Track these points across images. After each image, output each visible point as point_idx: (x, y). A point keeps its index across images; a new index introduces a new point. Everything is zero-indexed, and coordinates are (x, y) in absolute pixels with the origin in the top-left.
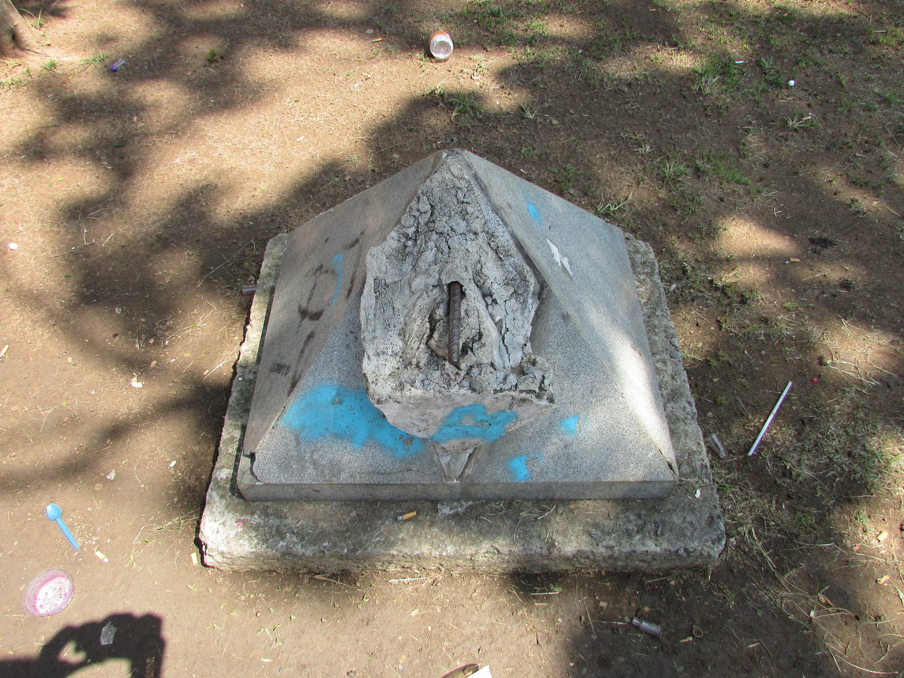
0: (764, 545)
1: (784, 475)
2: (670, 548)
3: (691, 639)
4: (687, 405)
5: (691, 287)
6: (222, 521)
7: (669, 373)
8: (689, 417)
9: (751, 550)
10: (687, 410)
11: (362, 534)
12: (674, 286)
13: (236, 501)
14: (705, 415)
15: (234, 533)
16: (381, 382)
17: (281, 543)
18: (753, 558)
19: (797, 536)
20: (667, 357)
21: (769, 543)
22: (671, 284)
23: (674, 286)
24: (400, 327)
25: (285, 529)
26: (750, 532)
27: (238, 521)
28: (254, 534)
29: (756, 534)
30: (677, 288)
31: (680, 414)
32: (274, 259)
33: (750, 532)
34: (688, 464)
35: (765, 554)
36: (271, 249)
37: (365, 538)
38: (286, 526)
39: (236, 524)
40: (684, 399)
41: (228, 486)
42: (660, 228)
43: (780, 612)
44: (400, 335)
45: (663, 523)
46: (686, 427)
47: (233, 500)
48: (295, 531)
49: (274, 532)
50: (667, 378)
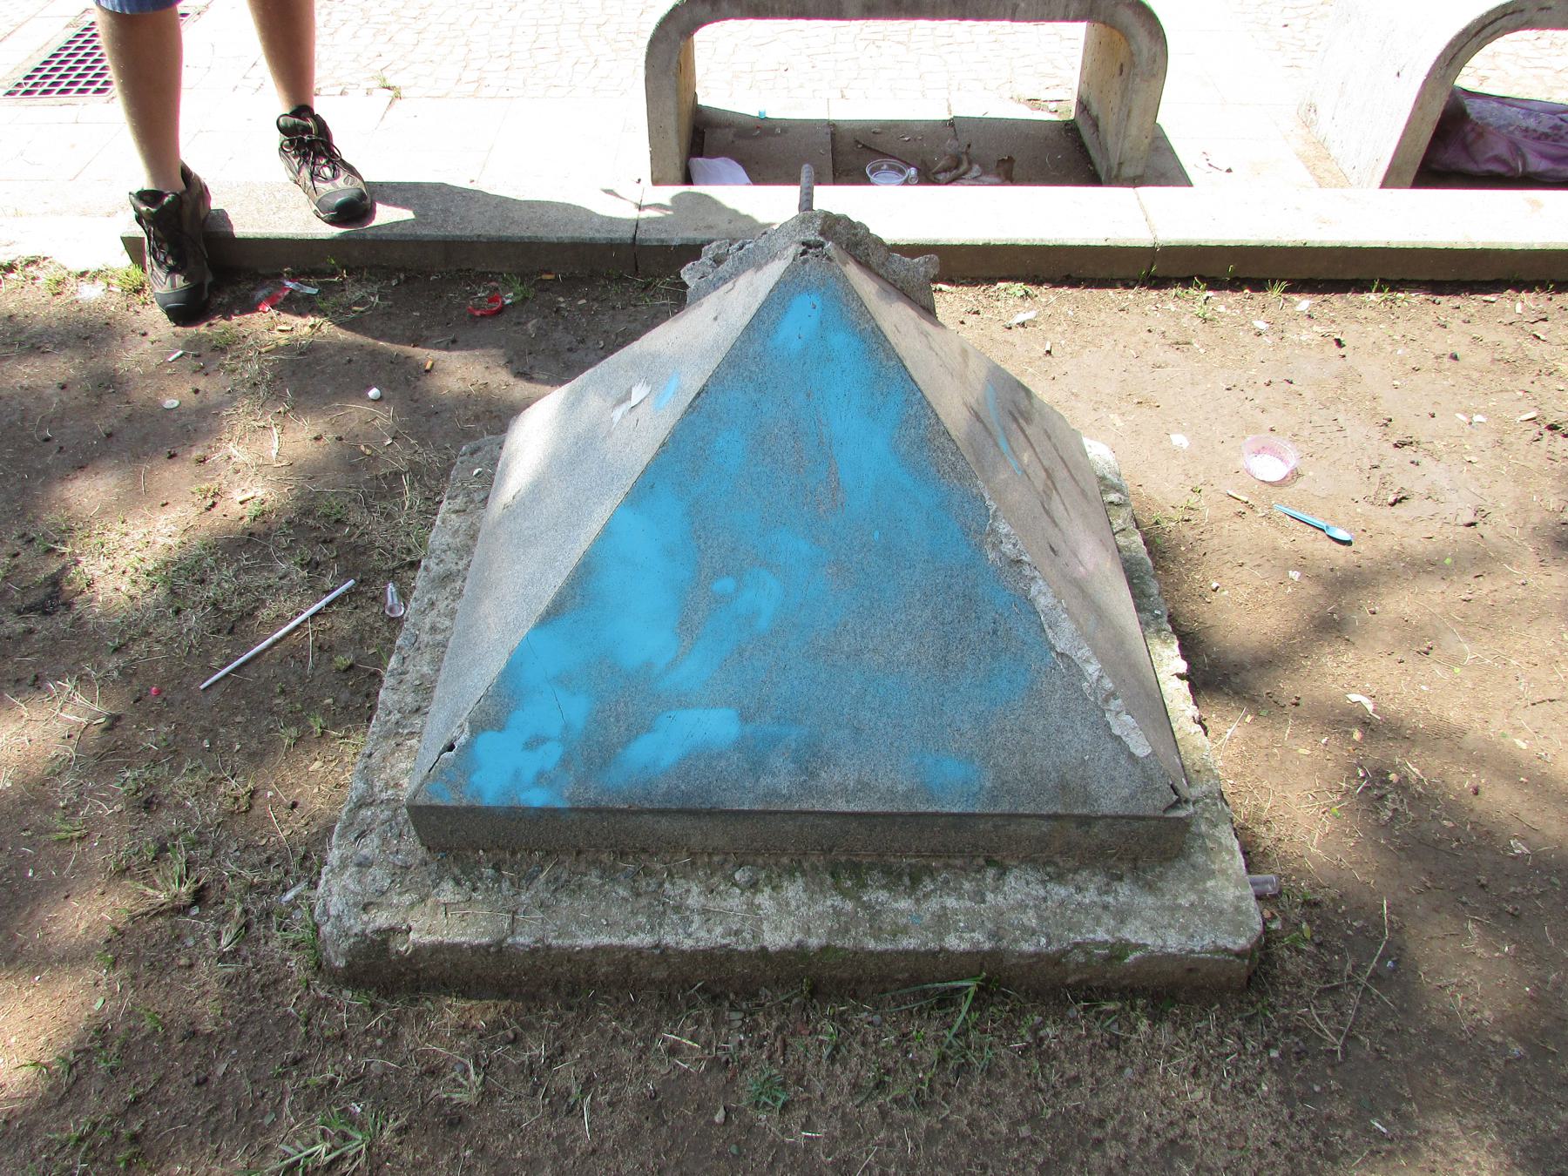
1: (318, 564)
5: (251, 887)
19: (355, 500)
20: (425, 638)
22: (293, 905)
23: (290, 895)
30: (285, 890)
32: (1223, 872)
34: (472, 501)
36: (1241, 898)
42: (222, 1069)
50: (441, 605)
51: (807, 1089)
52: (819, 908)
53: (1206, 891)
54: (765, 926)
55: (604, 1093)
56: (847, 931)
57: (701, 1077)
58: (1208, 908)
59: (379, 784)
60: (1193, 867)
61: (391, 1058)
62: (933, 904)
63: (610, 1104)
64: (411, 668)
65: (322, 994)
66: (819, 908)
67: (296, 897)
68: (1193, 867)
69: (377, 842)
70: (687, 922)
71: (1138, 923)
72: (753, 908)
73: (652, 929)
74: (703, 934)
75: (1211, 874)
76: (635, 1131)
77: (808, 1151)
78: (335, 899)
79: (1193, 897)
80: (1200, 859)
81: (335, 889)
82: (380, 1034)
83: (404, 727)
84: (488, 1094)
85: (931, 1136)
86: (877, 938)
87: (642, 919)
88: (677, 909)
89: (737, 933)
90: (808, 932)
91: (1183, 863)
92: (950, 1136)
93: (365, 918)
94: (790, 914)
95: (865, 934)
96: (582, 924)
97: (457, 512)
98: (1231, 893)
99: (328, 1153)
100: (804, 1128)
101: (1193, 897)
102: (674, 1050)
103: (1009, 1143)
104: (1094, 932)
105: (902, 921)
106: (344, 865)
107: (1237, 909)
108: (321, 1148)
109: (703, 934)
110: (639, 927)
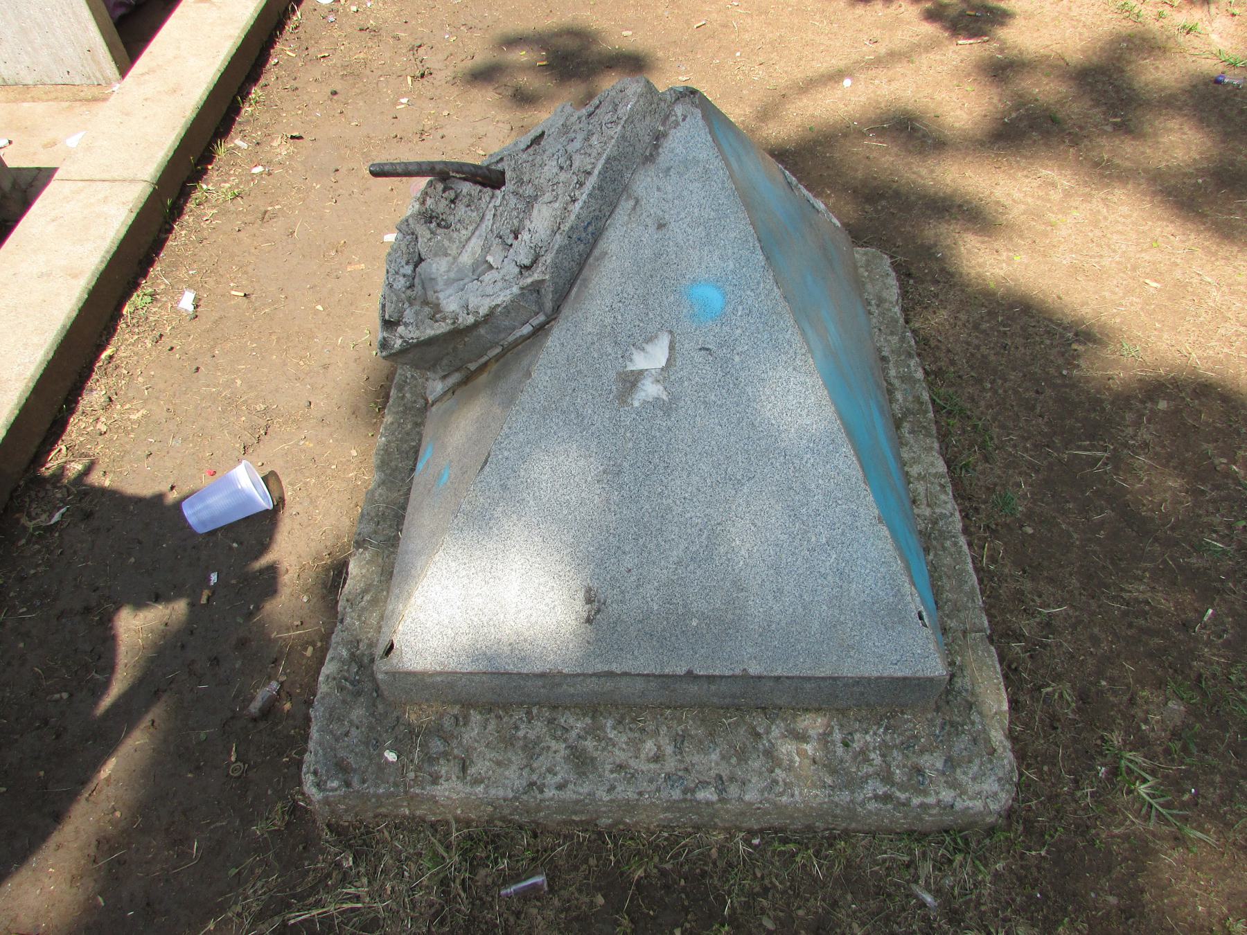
0: (331, 917)
2: (318, 696)
3: (233, 759)
4: (558, 779)
7: (632, 763)
8: (534, 777)
9: (328, 890)
10: (549, 776)
12: (928, 898)
14: (599, 889)
18: (313, 890)
20: (671, 764)
21: (331, 927)
22: (938, 893)
23: (928, 898)
26: (358, 898)
29: (353, 910)
30: (923, 905)
31: (542, 763)
33: (358, 898)
34: (445, 754)
35: (314, 912)
40: (572, 777)
43: (222, 908)
45: (358, 694)
46: (514, 767)
51: (995, 485)
52: (912, 441)
54: (933, 471)
55: (1033, 601)
57: (1005, 544)
59: (866, 769)
61: (1055, 756)
62: (896, 382)
63: (1040, 596)
64: (713, 773)
65: (1021, 828)
66: (912, 441)
67: (927, 888)
69: (926, 757)
70: (942, 516)
72: (920, 477)
74: (949, 506)
76: (1051, 580)
77: (1031, 485)
78: (986, 787)
81: (977, 788)
82: (1040, 771)
83: (792, 761)
84: (1058, 678)
85: (1002, 427)
86: (926, 412)
87: (948, 544)
88: (935, 523)
89: (943, 486)
90: (931, 448)
92: (1001, 418)
93: (1000, 750)
94: (919, 456)
96: (962, 582)
97: (464, 769)
99: (1144, 781)
102: (993, 559)
103: (996, 392)
105: (910, 398)
106: (953, 785)
108: (1142, 789)
109: (949, 506)
110: (955, 544)
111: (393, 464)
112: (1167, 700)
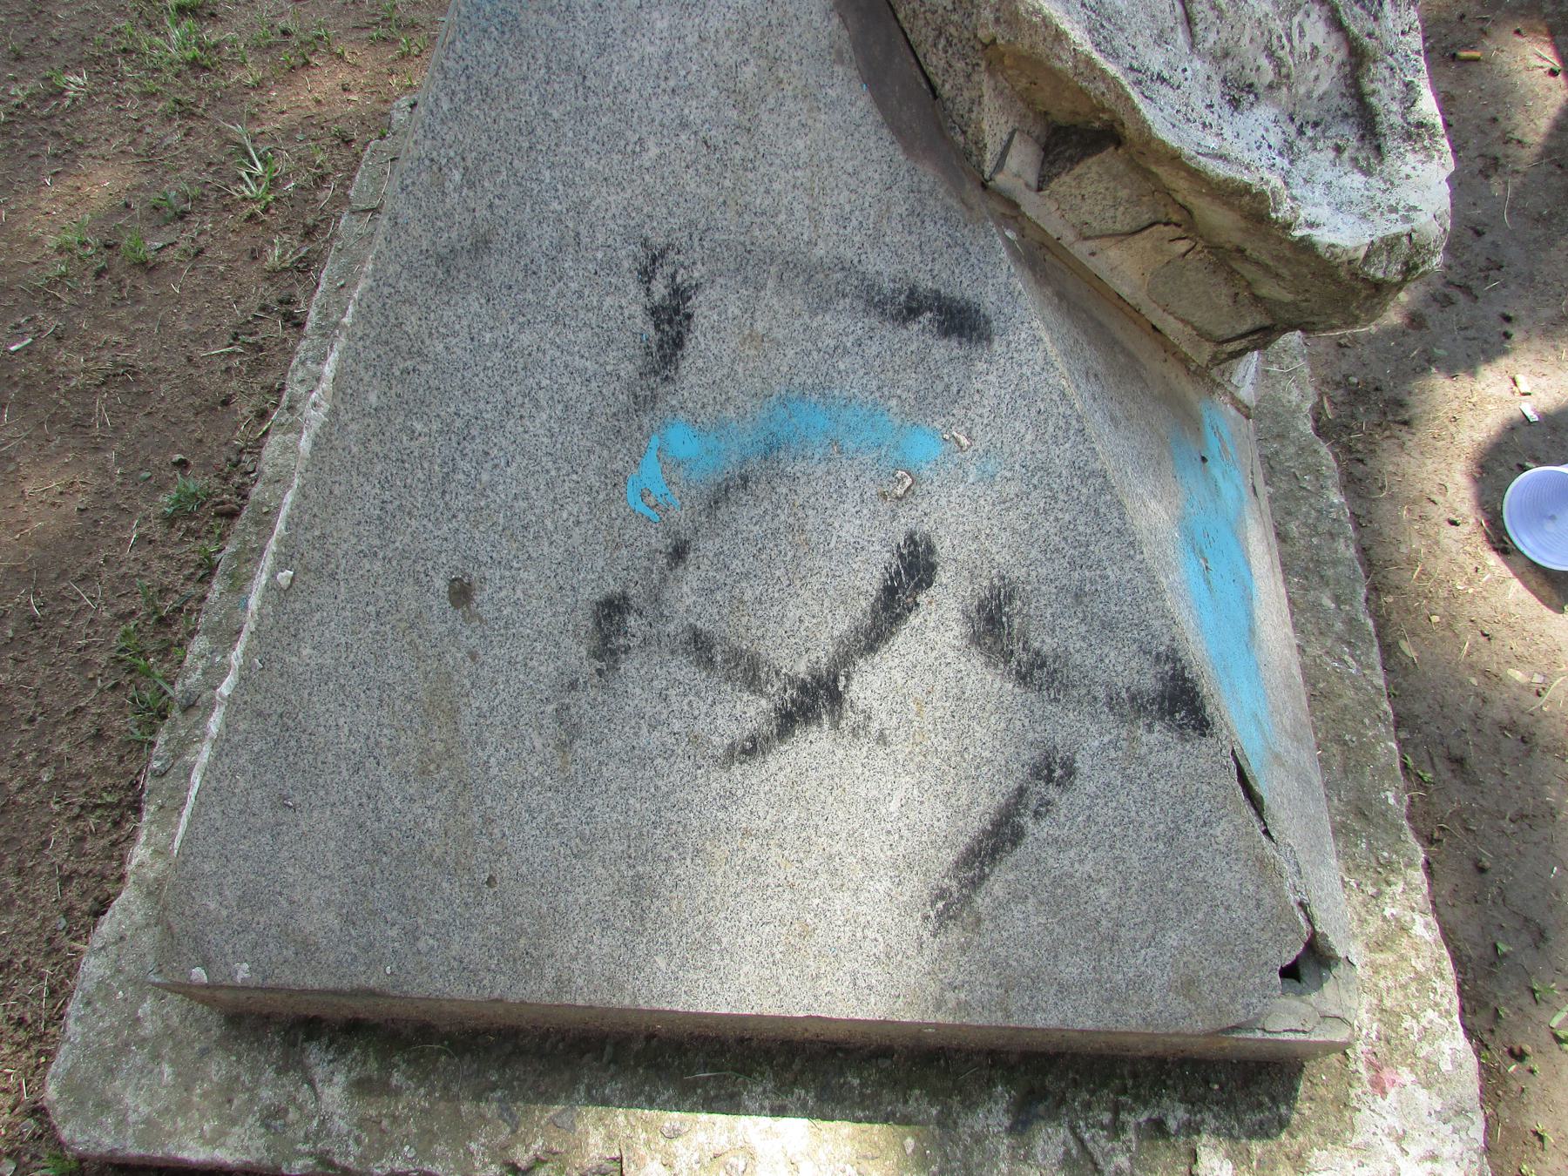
6: (1391, 1147)
11: (1341, 702)
13: (1305, 1107)
15: (1422, 1095)
16: (1406, 195)
17: (1418, 929)
24: (1216, 87)
25: (1374, 924)
27: (1379, 1086)
28: (1408, 1022)
32: (184, 1107)
36: (122, 1122)
37: (1351, 693)
38: (1362, 921)
39: (1392, 1092)
41: (1257, 1147)
44: (1235, 104)
47: (1305, 1120)
48: (1371, 890)
49: (1389, 957)
53: (156, 1057)
56: (257, 523)
58: (123, 1049)
60: (204, 1052)
68: (204, 1052)
71: (138, 918)
73: (321, 327)
74: (300, 374)
75: (186, 1080)
79: (148, 1028)
80: (217, 1069)
86: (236, 555)
91: (216, 1033)
95: (245, 542)
98: (136, 1103)
100: (141, 537)
101: (148, 1028)
104: (147, 844)
107: (104, 1105)
109: (300, 374)
111: (1292, 450)
112: (159, 250)
